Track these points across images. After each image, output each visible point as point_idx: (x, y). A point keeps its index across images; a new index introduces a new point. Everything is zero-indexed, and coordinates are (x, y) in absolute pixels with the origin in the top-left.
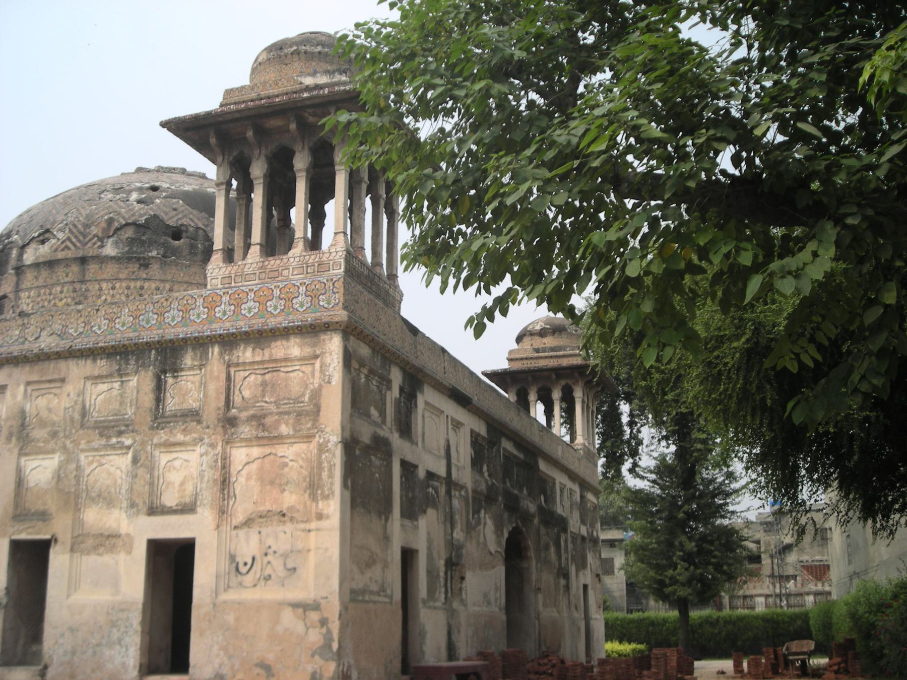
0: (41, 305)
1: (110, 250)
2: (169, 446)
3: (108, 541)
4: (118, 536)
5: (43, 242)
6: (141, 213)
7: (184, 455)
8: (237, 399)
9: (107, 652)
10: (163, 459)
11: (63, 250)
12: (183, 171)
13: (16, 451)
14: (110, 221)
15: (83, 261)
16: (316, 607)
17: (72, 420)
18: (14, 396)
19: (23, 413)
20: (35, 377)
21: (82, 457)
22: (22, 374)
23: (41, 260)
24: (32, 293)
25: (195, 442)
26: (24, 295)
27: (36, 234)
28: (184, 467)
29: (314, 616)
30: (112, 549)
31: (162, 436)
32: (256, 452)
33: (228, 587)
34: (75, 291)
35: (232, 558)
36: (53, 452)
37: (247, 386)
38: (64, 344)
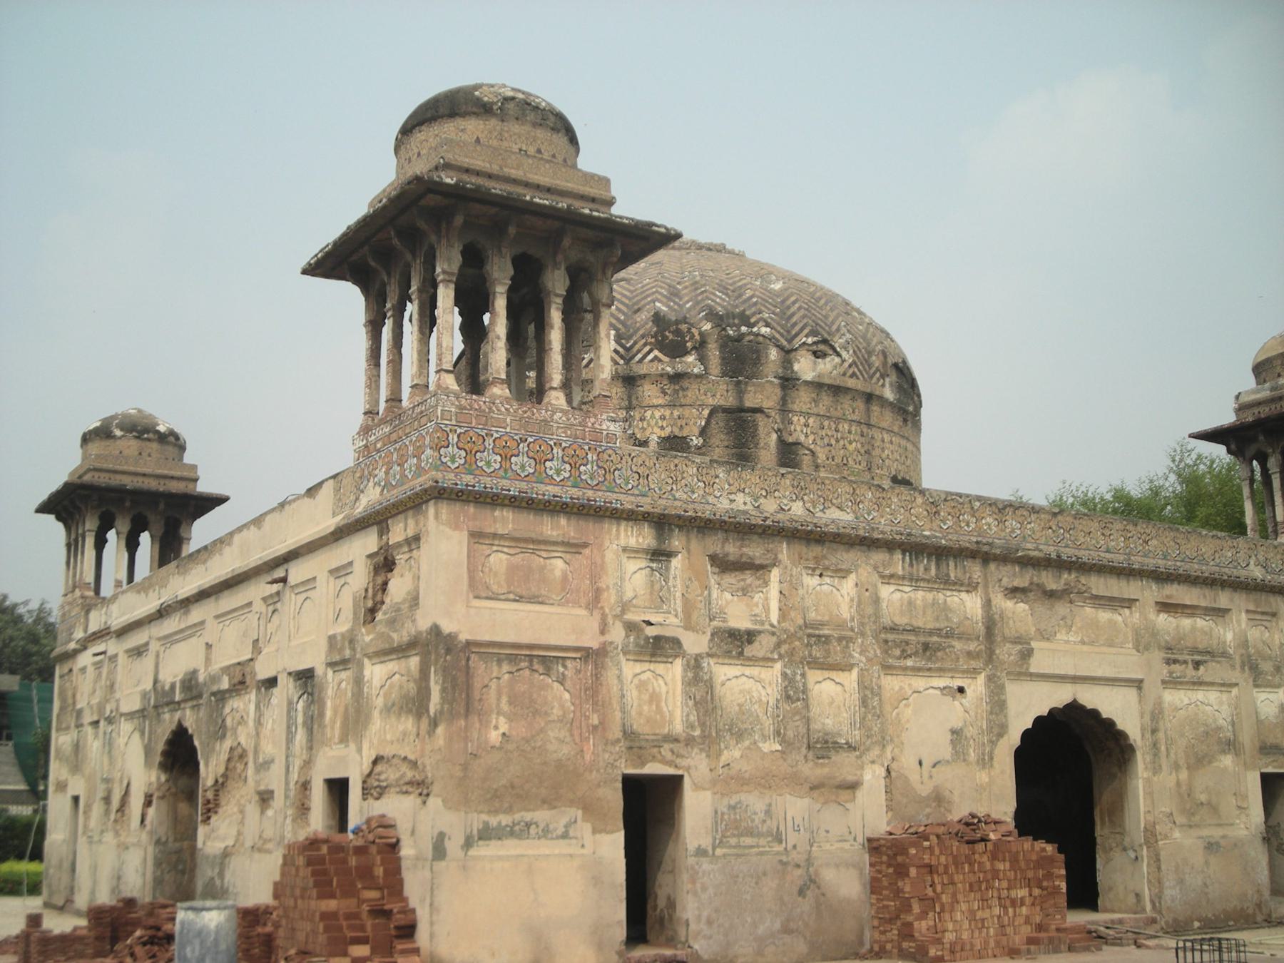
0: (826, 441)
1: (889, 394)
11: (851, 376)
13: (1251, 681)
15: (869, 398)
18: (1239, 622)
20: (1252, 607)
23: (827, 381)
24: (811, 421)
27: (810, 340)
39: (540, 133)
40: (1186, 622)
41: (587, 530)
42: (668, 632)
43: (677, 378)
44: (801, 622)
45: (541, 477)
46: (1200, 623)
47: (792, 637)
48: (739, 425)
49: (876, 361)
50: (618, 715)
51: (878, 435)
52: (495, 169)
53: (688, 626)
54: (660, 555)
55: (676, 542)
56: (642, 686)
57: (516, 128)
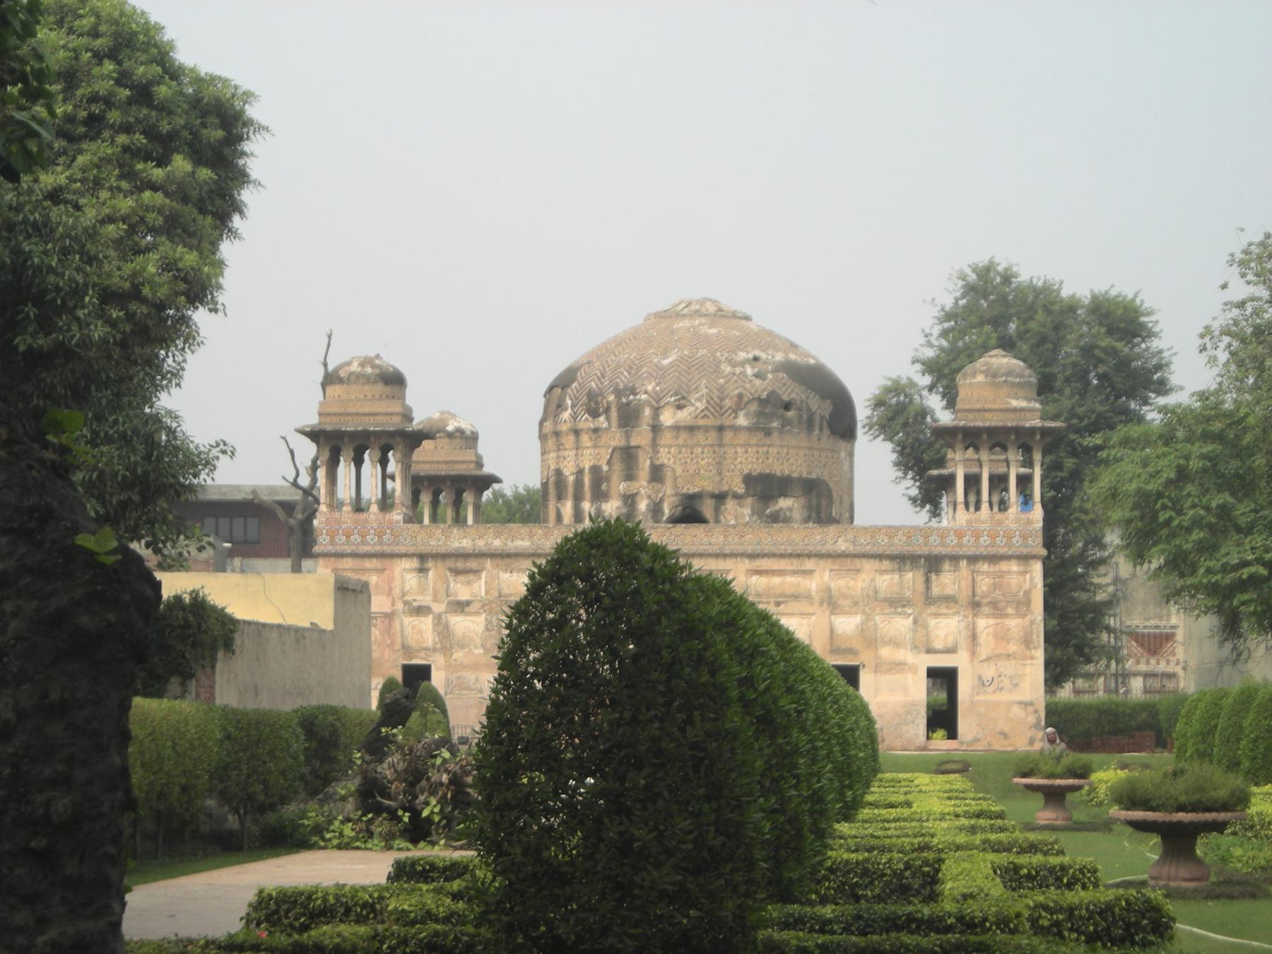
1: (742, 421)
2: (937, 615)
3: (898, 667)
4: (905, 664)
5: (680, 407)
6: (761, 387)
7: (947, 621)
8: (978, 591)
9: (905, 728)
10: (932, 622)
12: (734, 315)
14: (740, 396)
15: (721, 429)
16: (1031, 704)
17: (868, 595)
19: (830, 590)
21: (878, 619)
22: (826, 565)
23: (682, 424)
25: (954, 614)
26: (663, 451)
28: (946, 627)
29: (1031, 709)
30: (901, 671)
31: (933, 609)
32: (992, 621)
33: (978, 694)
34: (714, 452)
35: (980, 678)
36: (856, 613)
37: (984, 584)
38: (859, 550)
39: (367, 387)
40: (776, 580)
41: (387, 562)
42: (424, 604)
43: (596, 430)
44: (496, 594)
45: (364, 543)
46: (789, 579)
47: (490, 602)
48: (628, 455)
49: (728, 403)
50: (399, 640)
51: (731, 451)
52: (342, 410)
53: (435, 600)
54: (422, 570)
55: (430, 564)
56: (414, 627)
57: (354, 387)
